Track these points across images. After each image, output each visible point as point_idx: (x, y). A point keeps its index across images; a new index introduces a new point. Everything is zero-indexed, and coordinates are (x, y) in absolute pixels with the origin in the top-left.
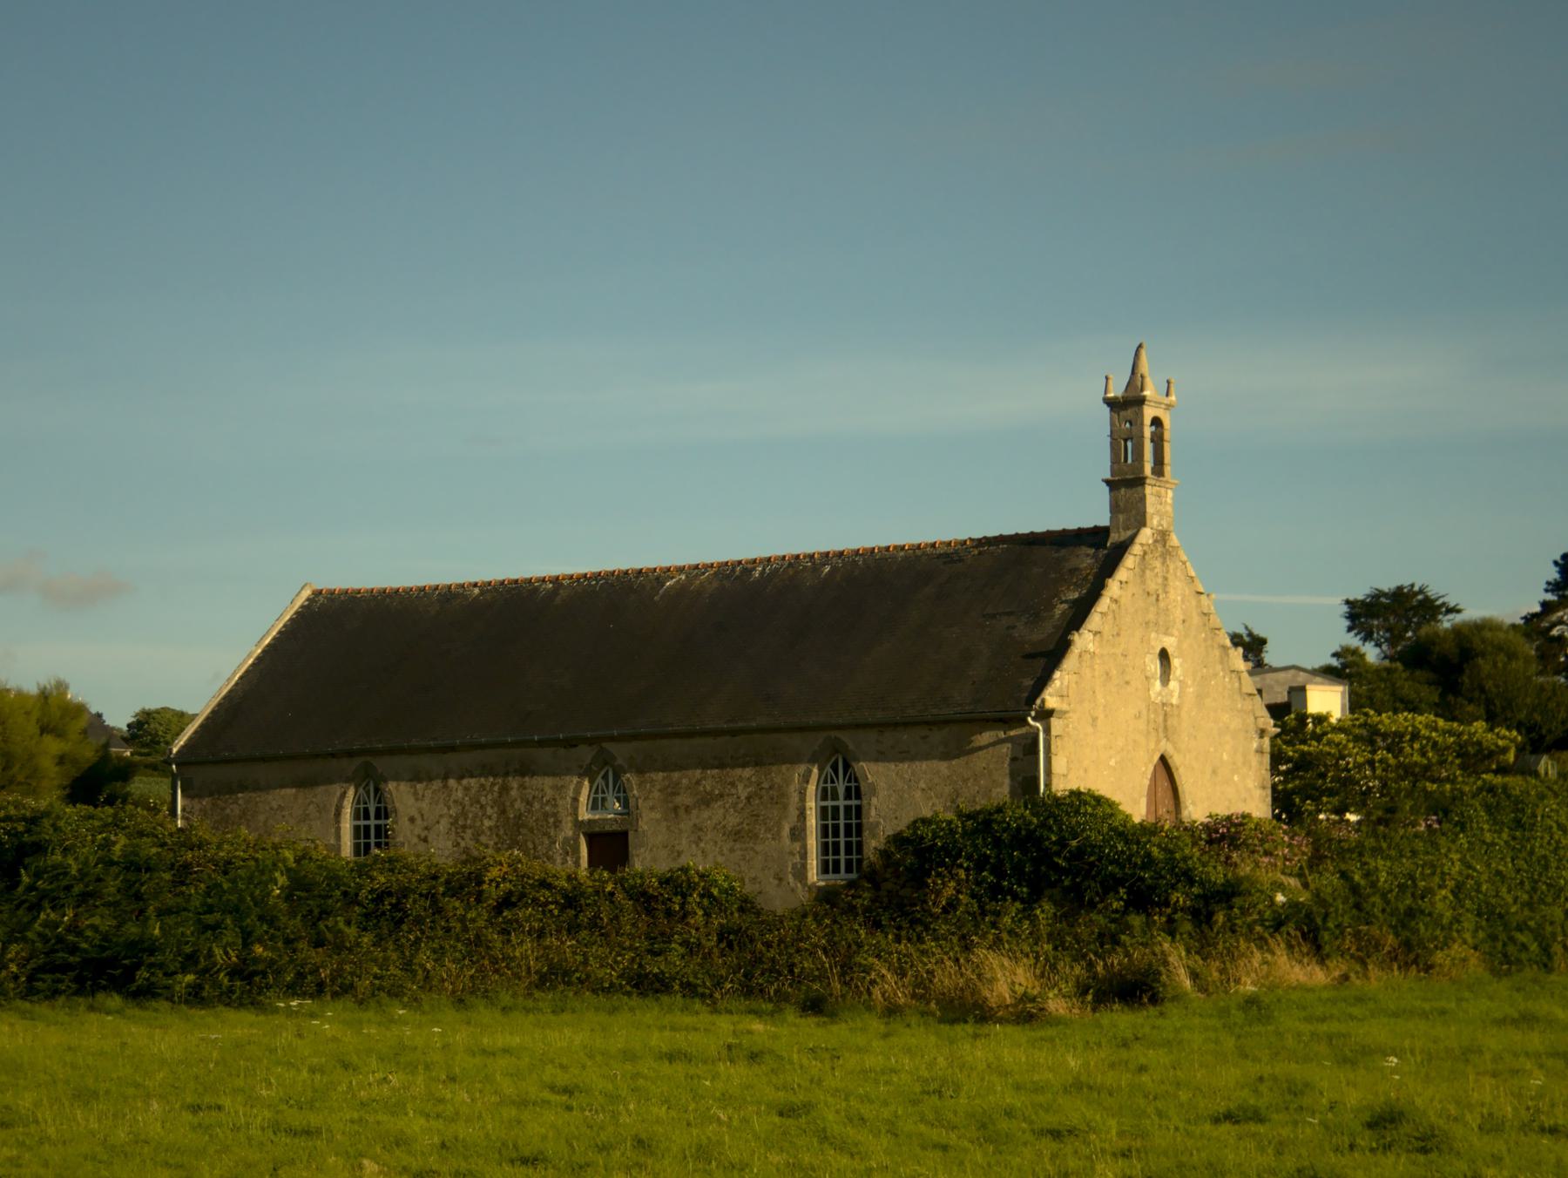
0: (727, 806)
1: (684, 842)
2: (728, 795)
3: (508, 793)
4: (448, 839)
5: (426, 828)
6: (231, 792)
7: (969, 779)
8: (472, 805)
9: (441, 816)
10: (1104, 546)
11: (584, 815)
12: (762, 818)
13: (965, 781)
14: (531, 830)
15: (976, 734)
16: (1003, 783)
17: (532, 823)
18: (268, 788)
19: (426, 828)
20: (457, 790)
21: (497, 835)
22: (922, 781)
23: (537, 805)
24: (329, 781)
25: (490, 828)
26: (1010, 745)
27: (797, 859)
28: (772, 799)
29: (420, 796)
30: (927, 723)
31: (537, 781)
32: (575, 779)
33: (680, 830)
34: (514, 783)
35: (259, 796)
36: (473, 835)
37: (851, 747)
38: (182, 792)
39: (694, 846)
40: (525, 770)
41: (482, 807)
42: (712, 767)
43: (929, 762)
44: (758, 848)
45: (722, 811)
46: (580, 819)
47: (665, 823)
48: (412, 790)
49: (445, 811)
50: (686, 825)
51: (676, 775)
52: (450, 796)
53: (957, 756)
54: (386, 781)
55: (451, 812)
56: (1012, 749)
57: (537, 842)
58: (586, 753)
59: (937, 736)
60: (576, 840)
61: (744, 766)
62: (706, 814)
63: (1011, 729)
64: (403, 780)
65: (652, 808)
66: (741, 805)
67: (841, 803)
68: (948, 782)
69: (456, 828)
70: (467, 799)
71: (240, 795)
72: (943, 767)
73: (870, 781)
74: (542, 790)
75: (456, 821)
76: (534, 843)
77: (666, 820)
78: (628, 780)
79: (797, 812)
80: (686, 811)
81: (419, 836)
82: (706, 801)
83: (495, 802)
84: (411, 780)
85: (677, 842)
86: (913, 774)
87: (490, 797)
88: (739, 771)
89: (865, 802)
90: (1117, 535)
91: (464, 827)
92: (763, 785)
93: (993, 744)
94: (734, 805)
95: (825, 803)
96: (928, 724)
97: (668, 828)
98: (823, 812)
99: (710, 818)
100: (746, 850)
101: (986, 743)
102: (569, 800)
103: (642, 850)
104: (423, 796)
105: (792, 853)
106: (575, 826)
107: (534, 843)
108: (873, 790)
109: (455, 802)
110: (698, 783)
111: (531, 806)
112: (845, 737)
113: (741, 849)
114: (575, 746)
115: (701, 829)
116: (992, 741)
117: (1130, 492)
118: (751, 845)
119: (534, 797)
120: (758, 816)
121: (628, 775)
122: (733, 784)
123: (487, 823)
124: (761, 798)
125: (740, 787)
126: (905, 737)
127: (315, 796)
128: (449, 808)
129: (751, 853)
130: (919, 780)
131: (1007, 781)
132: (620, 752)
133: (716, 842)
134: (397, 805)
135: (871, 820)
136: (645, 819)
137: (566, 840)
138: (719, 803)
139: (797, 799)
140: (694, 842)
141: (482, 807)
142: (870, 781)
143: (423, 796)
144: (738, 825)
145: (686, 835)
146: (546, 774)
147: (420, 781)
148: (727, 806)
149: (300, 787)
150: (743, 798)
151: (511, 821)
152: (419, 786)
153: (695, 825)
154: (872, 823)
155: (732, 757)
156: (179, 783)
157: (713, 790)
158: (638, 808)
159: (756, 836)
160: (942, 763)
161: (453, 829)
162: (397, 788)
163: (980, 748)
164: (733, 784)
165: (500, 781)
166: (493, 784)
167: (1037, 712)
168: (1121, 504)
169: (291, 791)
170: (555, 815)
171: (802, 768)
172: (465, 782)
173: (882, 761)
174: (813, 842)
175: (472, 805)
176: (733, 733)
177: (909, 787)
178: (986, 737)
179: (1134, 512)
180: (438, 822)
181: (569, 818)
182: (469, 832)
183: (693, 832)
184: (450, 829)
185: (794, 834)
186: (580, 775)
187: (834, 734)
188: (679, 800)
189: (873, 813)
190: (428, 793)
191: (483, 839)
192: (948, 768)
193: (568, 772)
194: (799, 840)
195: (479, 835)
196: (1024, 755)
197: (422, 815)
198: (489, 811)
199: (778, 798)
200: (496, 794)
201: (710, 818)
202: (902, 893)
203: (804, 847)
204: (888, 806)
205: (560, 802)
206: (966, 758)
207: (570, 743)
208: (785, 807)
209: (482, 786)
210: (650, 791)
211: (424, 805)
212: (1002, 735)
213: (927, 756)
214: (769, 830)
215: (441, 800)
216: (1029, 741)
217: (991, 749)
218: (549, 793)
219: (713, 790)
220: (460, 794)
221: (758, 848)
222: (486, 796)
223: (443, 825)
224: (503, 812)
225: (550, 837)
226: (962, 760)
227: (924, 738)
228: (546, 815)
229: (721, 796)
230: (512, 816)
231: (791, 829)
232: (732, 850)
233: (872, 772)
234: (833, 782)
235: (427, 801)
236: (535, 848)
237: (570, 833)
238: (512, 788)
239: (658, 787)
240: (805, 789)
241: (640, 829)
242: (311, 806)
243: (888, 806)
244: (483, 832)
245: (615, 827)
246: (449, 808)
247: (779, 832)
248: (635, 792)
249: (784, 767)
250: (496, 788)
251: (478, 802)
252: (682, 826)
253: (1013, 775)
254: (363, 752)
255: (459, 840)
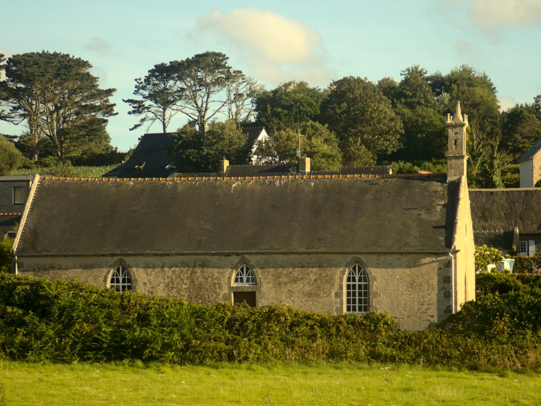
0: (305, 283)
1: (284, 297)
2: (305, 278)
3: (195, 274)
4: (164, 293)
5: (152, 288)
6: (45, 269)
7: (419, 276)
8: (176, 279)
9: (160, 283)
10: (446, 183)
11: (233, 284)
12: (321, 288)
13: (418, 276)
14: (207, 290)
15: (423, 258)
16: (434, 278)
17: (207, 287)
18: (67, 269)
19: (152, 288)
20: (168, 272)
21: (189, 291)
22: (398, 276)
23: (210, 280)
24: (101, 266)
25: (186, 289)
26: (438, 263)
27: (338, 305)
28: (326, 281)
29: (149, 274)
30: (401, 253)
31: (210, 270)
32: (230, 270)
33: (282, 292)
34: (198, 270)
35: (62, 272)
36: (177, 291)
37: (365, 261)
38: (18, 268)
39: (288, 299)
40: (203, 265)
41: (182, 279)
42: (298, 267)
43: (401, 269)
44: (320, 300)
45: (302, 285)
46: (232, 286)
47: (274, 289)
48: (145, 272)
49: (163, 280)
50: (285, 290)
51: (280, 270)
52: (165, 274)
53: (414, 267)
54: (131, 267)
55: (165, 281)
56: (439, 265)
57: (210, 295)
58: (235, 259)
59: (405, 258)
60: (230, 295)
61: (313, 267)
62: (295, 286)
63: (438, 257)
64: (140, 267)
65: (268, 283)
66: (311, 283)
67: (357, 283)
68: (410, 277)
69: (168, 288)
70: (173, 276)
71: (51, 271)
72: (407, 271)
73: (373, 275)
74: (213, 273)
75: (168, 285)
76: (208, 295)
77: (274, 287)
78: (256, 271)
79: (339, 286)
80: (285, 284)
81: (148, 291)
82: (295, 280)
83: (188, 278)
84: (144, 267)
85: (280, 297)
86: (394, 273)
87: (186, 275)
88: (311, 269)
89: (370, 283)
90: (450, 178)
91: (172, 288)
92: (323, 275)
93: (431, 263)
94: (308, 283)
95: (349, 283)
96: (401, 254)
97: (276, 291)
98: (348, 287)
99: (296, 287)
100: (314, 300)
101: (427, 262)
102: (226, 278)
103: (263, 299)
104: (151, 274)
105: (336, 303)
106: (229, 289)
107: (208, 295)
108: (375, 279)
109: (168, 277)
110: (291, 273)
111: (207, 280)
112: (362, 257)
113: (311, 301)
114: (231, 256)
115: (292, 292)
116: (430, 261)
117: (457, 161)
118: (316, 299)
119: (208, 276)
120: (320, 287)
121: (256, 269)
122: (308, 274)
123: (184, 286)
124: (321, 280)
125: (311, 275)
126: (390, 258)
127: (93, 272)
128: (164, 280)
129: (316, 302)
130: (396, 275)
131: (436, 277)
132: (253, 259)
133: (299, 297)
134: (137, 277)
135: (373, 290)
136: (264, 287)
137: (225, 295)
138: (301, 282)
139: (339, 281)
140: (288, 297)
141: (182, 279)
142: (373, 275)
143: (151, 274)
144: (310, 291)
145: (285, 294)
146: (214, 267)
147: (149, 268)
148: (305, 283)
149: (84, 268)
150: (313, 280)
151: (197, 286)
152: (148, 270)
153: (289, 290)
154: (374, 292)
155: (307, 263)
156: (16, 265)
157: (298, 276)
158: (261, 282)
159: (319, 295)
160: (406, 269)
161: (167, 288)
162: (137, 271)
163: (425, 264)
164: (308, 274)
165: (191, 269)
166: (187, 270)
167: (453, 251)
168: (453, 166)
169: (79, 270)
170: (219, 284)
171: (341, 269)
172: (173, 269)
173: (379, 268)
174: (345, 298)
175: (176, 279)
176: (309, 254)
177: (392, 278)
178: (427, 260)
179: (458, 169)
180: (159, 285)
181: (227, 286)
182: (175, 290)
183: (288, 293)
184: (165, 289)
185: (337, 295)
186: (232, 268)
187: (357, 256)
188: (281, 280)
189: (374, 288)
190: (154, 273)
191: (182, 293)
192: (410, 271)
193: (226, 266)
194: (339, 298)
195: (180, 291)
196: (444, 267)
197: (150, 282)
198: (185, 281)
199: (330, 281)
200: (189, 275)
201: (296, 287)
202: (474, 325)
203: (342, 300)
204: (381, 286)
205: (222, 279)
206: (418, 268)
207: (228, 255)
208: (333, 284)
209: (182, 270)
210: (267, 276)
211: (152, 278)
212: (434, 259)
213: (400, 266)
214: (325, 293)
215: (160, 276)
216: (447, 262)
217: (429, 265)
218: (216, 275)
219: (298, 276)
220: (170, 274)
221: (320, 300)
222: (184, 275)
223: (162, 286)
224: (193, 282)
225: (216, 293)
226: (416, 269)
227: (399, 259)
228: (215, 284)
229: (302, 279)
230: (197, 284)
231: (335, 293)
232: (307, 301)
233: (374, 272)
234: (353, 274)
235: (153, 276)
236: (209, 297)
237: (227, 292)
238: (197, 272)
239: (271, 274)
240: (343, 277)
241: (262, 291)
242: (91, 277)
243: (381, 286)
244: (182, 290)
245: (249, 290)
246: (164, 280)
247: (330, 294)
248: (260, 276)
249: (333, 269)
250: (189, 272)
251: (180, 277)
252: (283, 290)
253: (439, 275)
254: (120, 255)
255: (170, 293)
